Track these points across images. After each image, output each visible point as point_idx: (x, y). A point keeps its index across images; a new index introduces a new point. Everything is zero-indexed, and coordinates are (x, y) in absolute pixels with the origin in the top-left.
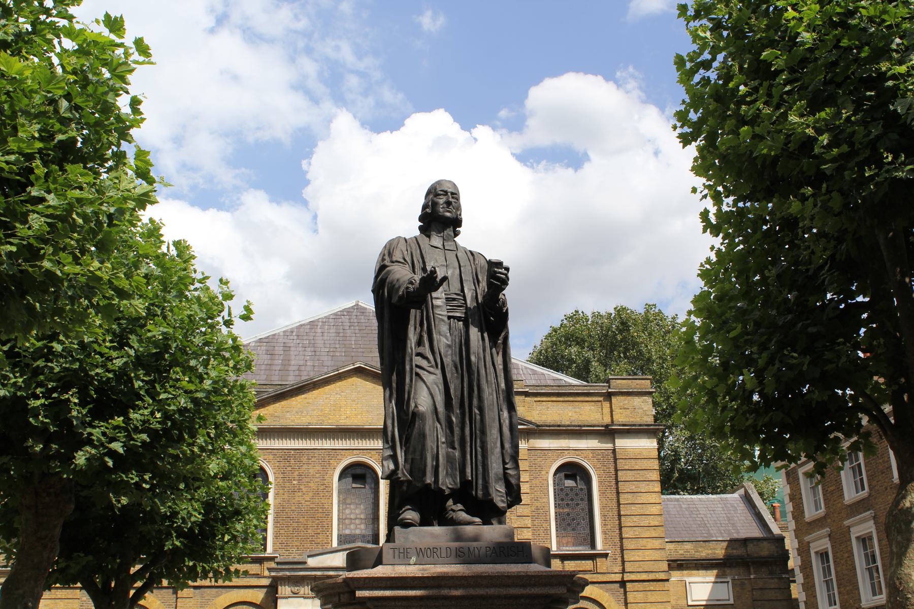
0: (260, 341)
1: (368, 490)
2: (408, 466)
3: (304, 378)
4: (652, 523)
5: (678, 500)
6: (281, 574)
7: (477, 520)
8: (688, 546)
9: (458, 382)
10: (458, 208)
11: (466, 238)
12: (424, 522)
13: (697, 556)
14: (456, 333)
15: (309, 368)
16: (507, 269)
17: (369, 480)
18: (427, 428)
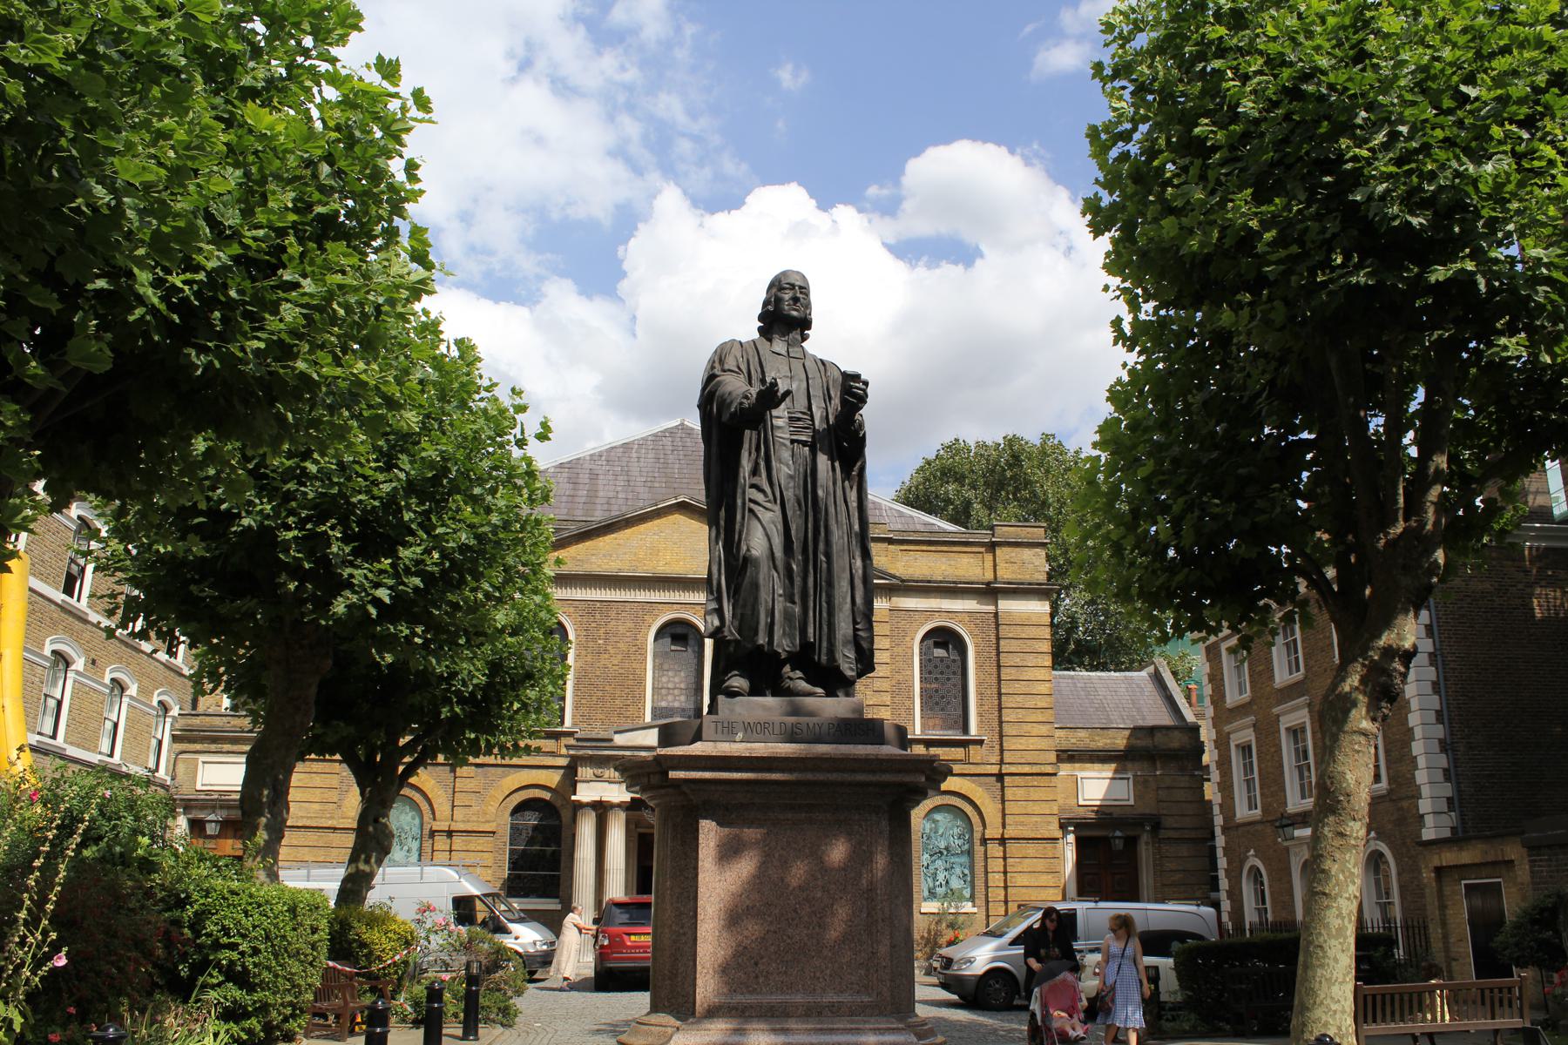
1: (690, 654)
2: (736, 623)
3: (614, 513)
4: (1040, 705)
5: (1072, 677)
6: (581, 752)
7: (819, 690)
8: (1082, 734)
9: (801, 521)
10: (808, 306)
11: (817, 344)
12: (754, 691)
13: (1093, 746)
14: (800, 461)
15: (621, 502)
16: (866, 383)
17: (691, 642)
18: (761, 577)
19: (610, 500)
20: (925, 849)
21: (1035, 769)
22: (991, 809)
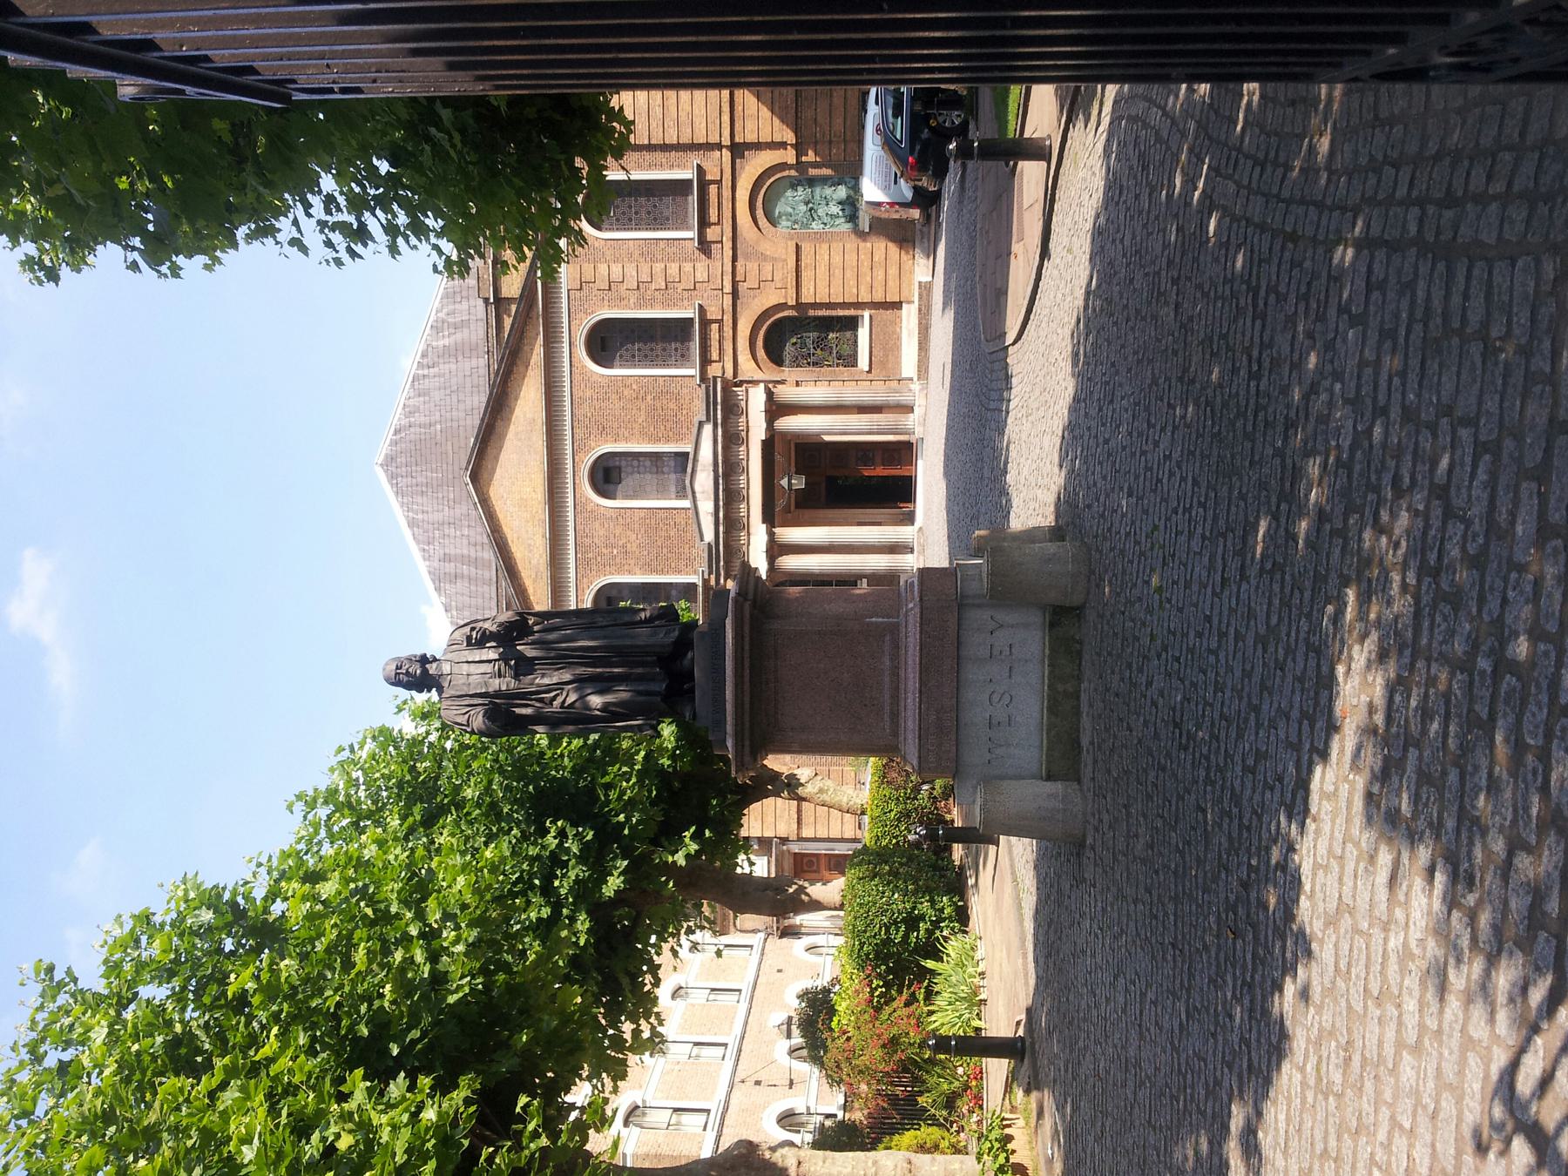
0: (438, 589)
3: (486, 540)
7: (690, 655)
15: (472, 533)
17: (611, 464)
19: (471, 538)
20: (807, 226)
21: (726, 108)
22: (767, 159)
